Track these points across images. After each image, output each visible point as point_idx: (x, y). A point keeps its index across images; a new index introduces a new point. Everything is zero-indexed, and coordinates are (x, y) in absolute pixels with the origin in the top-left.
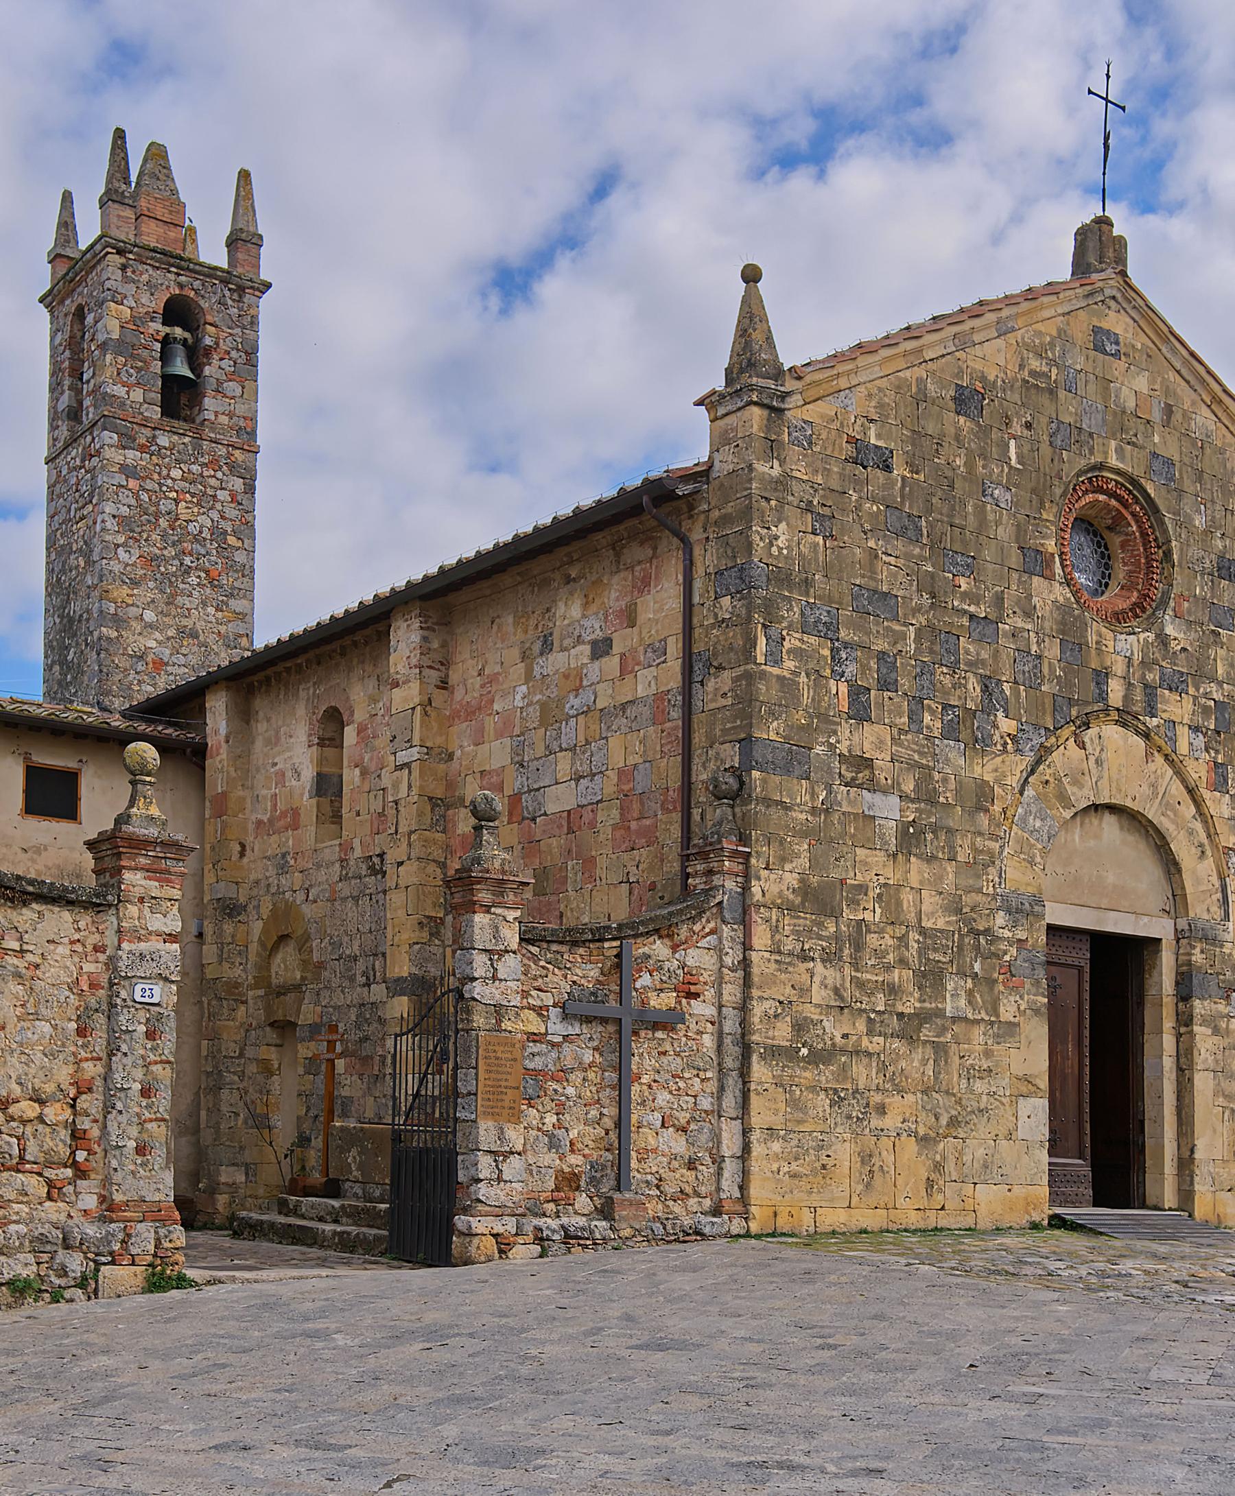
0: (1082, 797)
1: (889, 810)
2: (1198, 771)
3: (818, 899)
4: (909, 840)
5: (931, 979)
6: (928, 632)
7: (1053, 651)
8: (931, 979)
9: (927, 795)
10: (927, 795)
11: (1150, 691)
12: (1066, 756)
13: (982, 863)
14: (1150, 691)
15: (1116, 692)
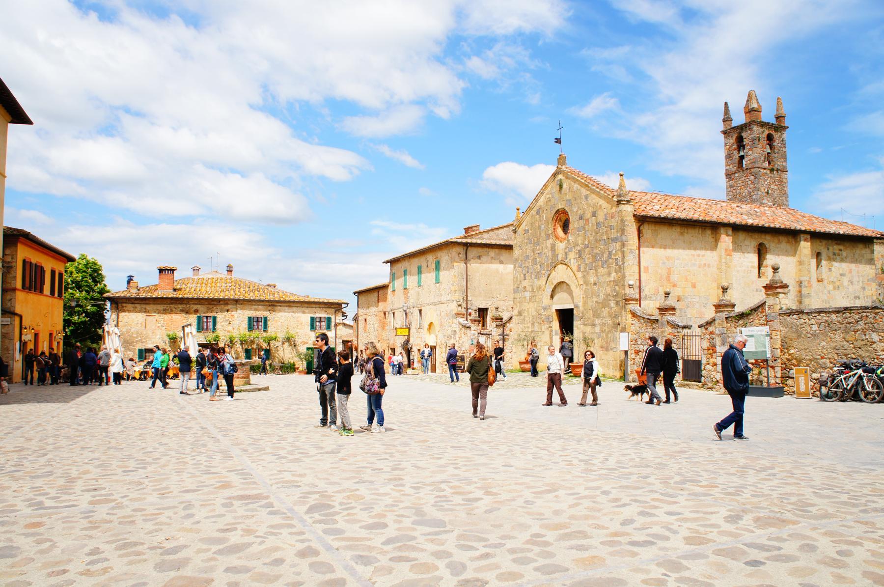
0: (555, 283)
1: (528, 295)
2: (575, 268)
3: (520, 313)
4: (530, 299)
5: (533, 324)
6: (533, 260)
7: (550, 254)
8: (533, 324)
9: (533, 291)
10: (533, 291)
11: (566, 253)
12: (553, 274)
13: (541, 300)
14: (566, 253)
15: (560, 258)
